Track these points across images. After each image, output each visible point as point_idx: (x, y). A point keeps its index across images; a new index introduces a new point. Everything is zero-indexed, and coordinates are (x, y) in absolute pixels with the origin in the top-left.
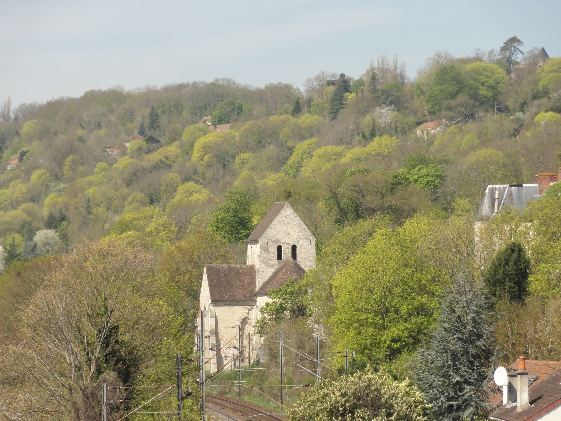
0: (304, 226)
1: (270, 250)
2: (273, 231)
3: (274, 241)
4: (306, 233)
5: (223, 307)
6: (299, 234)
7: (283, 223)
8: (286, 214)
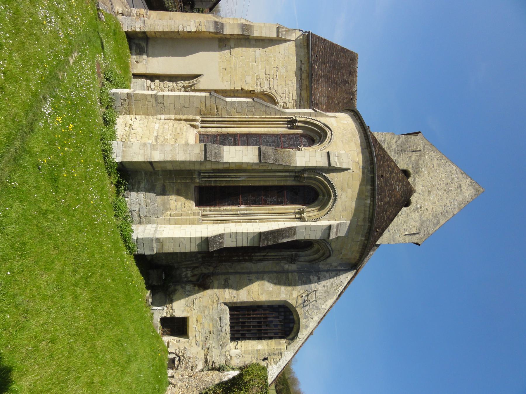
0: (443, 222)
1: (403, 155)
2: (435, 162)
3: (417, 163)
4: (431, 225)
5: (294, 59)
6: (430, 211)
7: (449, 181)
8: (464, 187)
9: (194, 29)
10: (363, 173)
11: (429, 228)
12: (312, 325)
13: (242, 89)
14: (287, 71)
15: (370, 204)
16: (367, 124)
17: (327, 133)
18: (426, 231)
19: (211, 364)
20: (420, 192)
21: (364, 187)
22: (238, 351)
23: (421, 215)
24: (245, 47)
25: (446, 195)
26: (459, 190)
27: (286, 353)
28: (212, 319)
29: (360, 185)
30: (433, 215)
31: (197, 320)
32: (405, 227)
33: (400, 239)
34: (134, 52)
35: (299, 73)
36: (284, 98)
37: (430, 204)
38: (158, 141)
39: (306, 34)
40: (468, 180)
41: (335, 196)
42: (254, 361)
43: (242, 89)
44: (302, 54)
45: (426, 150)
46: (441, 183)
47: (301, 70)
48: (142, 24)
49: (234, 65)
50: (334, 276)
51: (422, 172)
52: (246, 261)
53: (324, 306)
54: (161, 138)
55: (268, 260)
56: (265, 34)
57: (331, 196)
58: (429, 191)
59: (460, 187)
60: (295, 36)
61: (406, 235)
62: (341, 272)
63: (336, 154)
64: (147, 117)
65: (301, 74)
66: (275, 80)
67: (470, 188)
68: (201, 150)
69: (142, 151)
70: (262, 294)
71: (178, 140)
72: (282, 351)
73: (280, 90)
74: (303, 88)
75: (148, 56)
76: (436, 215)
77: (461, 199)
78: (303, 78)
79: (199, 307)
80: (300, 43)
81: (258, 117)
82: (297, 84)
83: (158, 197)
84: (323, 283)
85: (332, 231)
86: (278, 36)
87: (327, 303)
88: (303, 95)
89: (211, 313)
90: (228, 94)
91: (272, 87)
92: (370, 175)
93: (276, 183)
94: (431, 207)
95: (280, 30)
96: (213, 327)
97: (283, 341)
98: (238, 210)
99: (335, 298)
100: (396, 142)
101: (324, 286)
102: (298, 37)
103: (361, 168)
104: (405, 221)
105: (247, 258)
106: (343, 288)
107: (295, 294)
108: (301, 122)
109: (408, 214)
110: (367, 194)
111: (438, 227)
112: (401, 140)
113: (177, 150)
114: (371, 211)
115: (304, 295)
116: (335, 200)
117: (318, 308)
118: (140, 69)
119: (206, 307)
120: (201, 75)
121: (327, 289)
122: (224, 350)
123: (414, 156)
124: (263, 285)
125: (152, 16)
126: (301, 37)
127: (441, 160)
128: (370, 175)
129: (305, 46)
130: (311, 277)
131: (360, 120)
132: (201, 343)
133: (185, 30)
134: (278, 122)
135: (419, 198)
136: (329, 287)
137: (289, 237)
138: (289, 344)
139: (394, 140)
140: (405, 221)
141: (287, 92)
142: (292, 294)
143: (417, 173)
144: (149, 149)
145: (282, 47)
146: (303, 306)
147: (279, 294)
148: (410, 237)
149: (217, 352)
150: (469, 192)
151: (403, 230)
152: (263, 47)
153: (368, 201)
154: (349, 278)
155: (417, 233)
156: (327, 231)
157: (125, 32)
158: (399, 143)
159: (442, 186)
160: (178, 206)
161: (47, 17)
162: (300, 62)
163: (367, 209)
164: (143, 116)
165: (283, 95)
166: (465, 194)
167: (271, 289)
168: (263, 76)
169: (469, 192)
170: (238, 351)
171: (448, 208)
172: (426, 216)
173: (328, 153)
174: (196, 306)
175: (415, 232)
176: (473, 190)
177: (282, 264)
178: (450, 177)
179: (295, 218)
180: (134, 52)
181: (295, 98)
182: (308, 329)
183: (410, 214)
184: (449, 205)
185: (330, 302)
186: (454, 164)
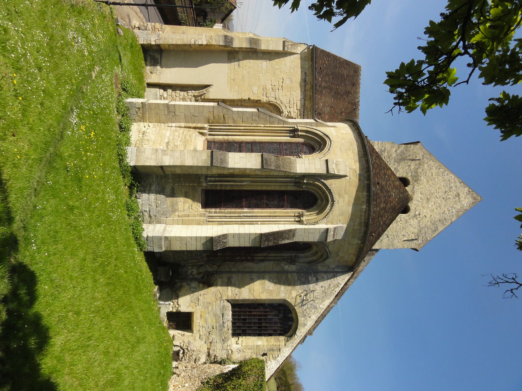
0: (441, 229)
1: (402, 164)
2: (434, 171)
3: (416, 172)
4: (430, 232)
7: (447, 189)
8: (462, 196)
9: (205, 43)
10: (360, 180)
11: (427, 235)
12: (310, 323)
13: (249, 99)
14: (291, 82)
15: (366, 209)
16: (365, 132)
17: (326, 142)
18: (424, 238)
19: (213, 357)
20: (419, 199)
21: (360, 193)
22: (239, 346)
23: (419, 222)
24: (253, 59)
25: (444, 203)
26: (457, 198)
27: (284, 349)
28: (215, 315)
29: (357, 191)
30: (431, 222)
31: (201, 316)
32: (403, 233)
33: (398, 245)
34: (148, 63)
35: (303, 84)
36: (288, 108)
37: (428, 211)
38: (169, 147)
39: (311, 47)
40: (466, 189)
41: (333, 201)
42: (254, 356)
43: (249, 99)
44: (307, 66)
45: (425, 159)
46: (440, 191)
47: (305, 81)
48: (157, 38)
49: (242, 76)
50: (332, 278)
51: (421, 180)
52: (248, 261)
53: (321, 306)
54: (171, 144)
55: (269, 260)
56: (271, 47)
57: (329, 201)
58: (427, 199)
59: (459, 195)
60: (300, 49)
61: (405, 241)
62: (339, 274)
63: (335, 161)
64: (159, 124)
65: (305, 86)
66: (281, 91)
67: (468, 196)
68: (208, 156)
69: (154, 156)
70: (263, 293)
71: (187, 146)
72: (281, 347)
73: (285, 100)
75: (161, 67)
76: (434, 222)
77: (459, 207)
79: (203, 303)
81: (262, 126)
82: (301, 95)
83: (167, 199)
84: (321, 284)
85: (329, 234)
86: (284, 49)
87: (324, 303)
88: (306, 105)
89: (214, 309)
90: (236, 103)
91: (277, 97)
92: (366, 182)
93: (277, 188)
94: (430, 214)
95: (286, 44)
96: (216, 322)
97: (282, 338)
98: (241, 213)
99: (332, 298)
100: (396, 151)
101: (322, 287)
102: (303, 51)
103: (358, 175)
104: (403, 228)
105: (249, 258)
106: (340, 289)
107: (294, 294)
108: (302, 131)
109: (406, 220)
110: (363, 200)
111: (436, 234)
112: (400, 149)
113: (186, 156)
114: (367, 216)
115: (302, 295)
116: (332, 205)
117: (315, 308)
118: (153, 79)
119: (210, 303)
120: (210, 85)
121: (325, 290)
122: (226, 344)
123: (413, 165)
124: (264, 284)
125: (166, 30)
126: (306, 51)
127: (439, 169)
128: (366, 182)
129: (310, 59)
130: (310, 278)
131: (359, 130)
132: (204, 338)
133: (197, 43)
134: (281, 131)
135: (418, 205)
136: (327, 287)
137: (288, 239)
138: (288, 341)
139: (394, 149)
140: (403, 228)
141: (292, 102)
142: (291, 293)
143: (416, 181)
144: (160, 154)
145: (288, 59)
146: (302, 305)
147: (279, 293)
148: (408, 243)
149: (219, 346)
150: (467, 200)
151: (402, 236)
152: (270, 60)
153: (364, 207)
154: (346, 280)
155: (416, 239)
156: (325, 234)
157: (141, 45)
158: (398, 152)
159: (440, 194)
160: (185, 208)
161: (75, 38)
163: (363, 214)
164: (156, 124)
165: (287, 105)
166: (463, 203)
167: (271, 288)
168: (269, 87)
169: (467, 200)
170: (239, 346)
171: (446, 216)
172: (424, 223)
173: (327, 161)
174: (201, 302)
175: (414, 238)
176: (471, 199)
177: (282, 265)
178: (449, 185)
179: (295, 221)
180: (148, 63)
181: (299, 108)
182: (306, 327)
183: (409, 221)
184: (447, 212)
185: (327, 302)
186: (453, 173)
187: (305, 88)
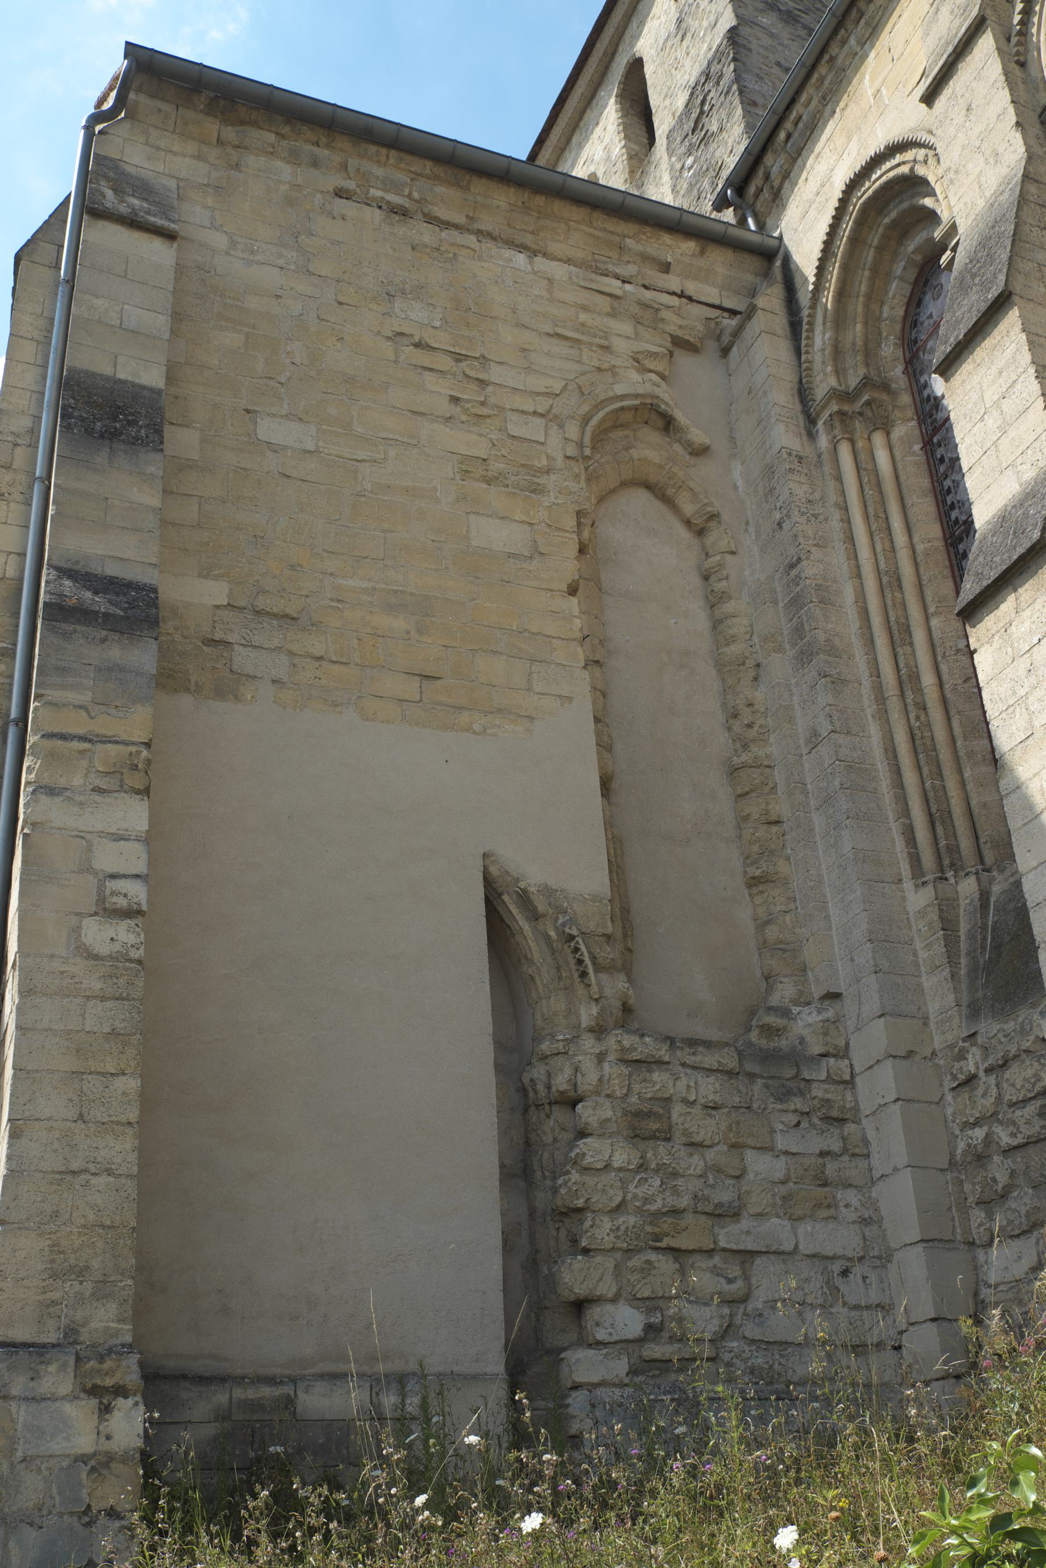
48: (58, 1379)
65: (431, 220)
74: (528, 240)
78: (460, 219)
80: (199, 157)
120: (488, 881)
129: (230, 133)
162: (341, 205)
165: (591, 358)
168: (469, 442)
187: (447, 225)
